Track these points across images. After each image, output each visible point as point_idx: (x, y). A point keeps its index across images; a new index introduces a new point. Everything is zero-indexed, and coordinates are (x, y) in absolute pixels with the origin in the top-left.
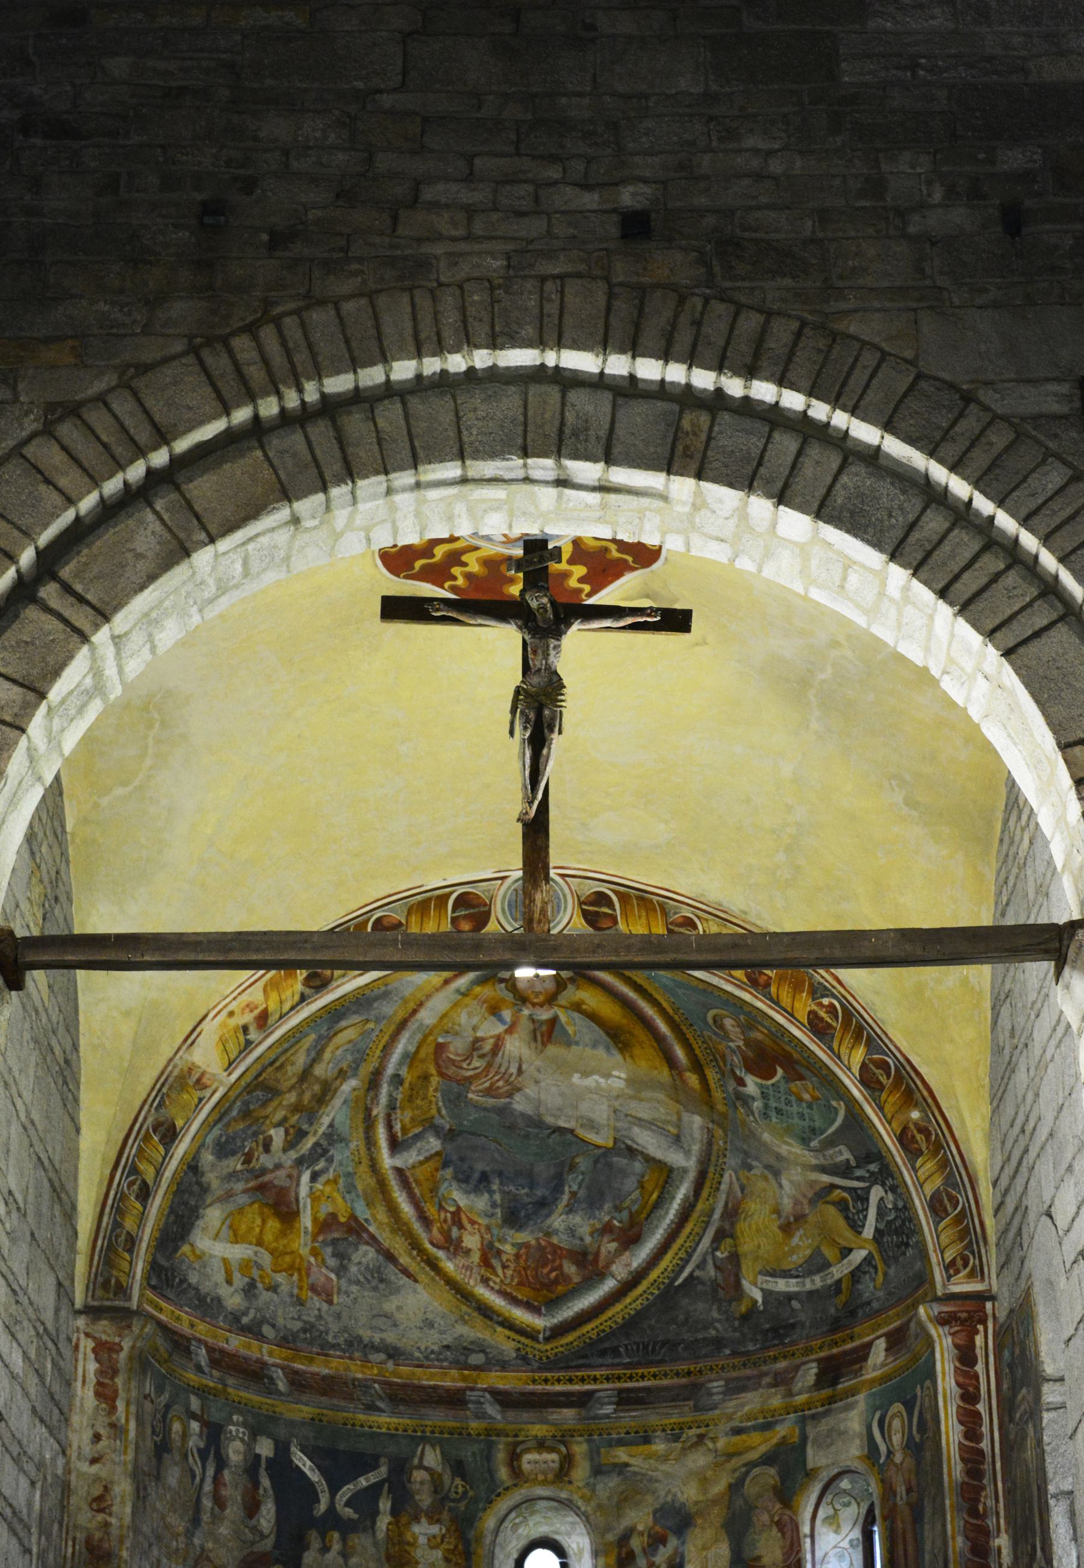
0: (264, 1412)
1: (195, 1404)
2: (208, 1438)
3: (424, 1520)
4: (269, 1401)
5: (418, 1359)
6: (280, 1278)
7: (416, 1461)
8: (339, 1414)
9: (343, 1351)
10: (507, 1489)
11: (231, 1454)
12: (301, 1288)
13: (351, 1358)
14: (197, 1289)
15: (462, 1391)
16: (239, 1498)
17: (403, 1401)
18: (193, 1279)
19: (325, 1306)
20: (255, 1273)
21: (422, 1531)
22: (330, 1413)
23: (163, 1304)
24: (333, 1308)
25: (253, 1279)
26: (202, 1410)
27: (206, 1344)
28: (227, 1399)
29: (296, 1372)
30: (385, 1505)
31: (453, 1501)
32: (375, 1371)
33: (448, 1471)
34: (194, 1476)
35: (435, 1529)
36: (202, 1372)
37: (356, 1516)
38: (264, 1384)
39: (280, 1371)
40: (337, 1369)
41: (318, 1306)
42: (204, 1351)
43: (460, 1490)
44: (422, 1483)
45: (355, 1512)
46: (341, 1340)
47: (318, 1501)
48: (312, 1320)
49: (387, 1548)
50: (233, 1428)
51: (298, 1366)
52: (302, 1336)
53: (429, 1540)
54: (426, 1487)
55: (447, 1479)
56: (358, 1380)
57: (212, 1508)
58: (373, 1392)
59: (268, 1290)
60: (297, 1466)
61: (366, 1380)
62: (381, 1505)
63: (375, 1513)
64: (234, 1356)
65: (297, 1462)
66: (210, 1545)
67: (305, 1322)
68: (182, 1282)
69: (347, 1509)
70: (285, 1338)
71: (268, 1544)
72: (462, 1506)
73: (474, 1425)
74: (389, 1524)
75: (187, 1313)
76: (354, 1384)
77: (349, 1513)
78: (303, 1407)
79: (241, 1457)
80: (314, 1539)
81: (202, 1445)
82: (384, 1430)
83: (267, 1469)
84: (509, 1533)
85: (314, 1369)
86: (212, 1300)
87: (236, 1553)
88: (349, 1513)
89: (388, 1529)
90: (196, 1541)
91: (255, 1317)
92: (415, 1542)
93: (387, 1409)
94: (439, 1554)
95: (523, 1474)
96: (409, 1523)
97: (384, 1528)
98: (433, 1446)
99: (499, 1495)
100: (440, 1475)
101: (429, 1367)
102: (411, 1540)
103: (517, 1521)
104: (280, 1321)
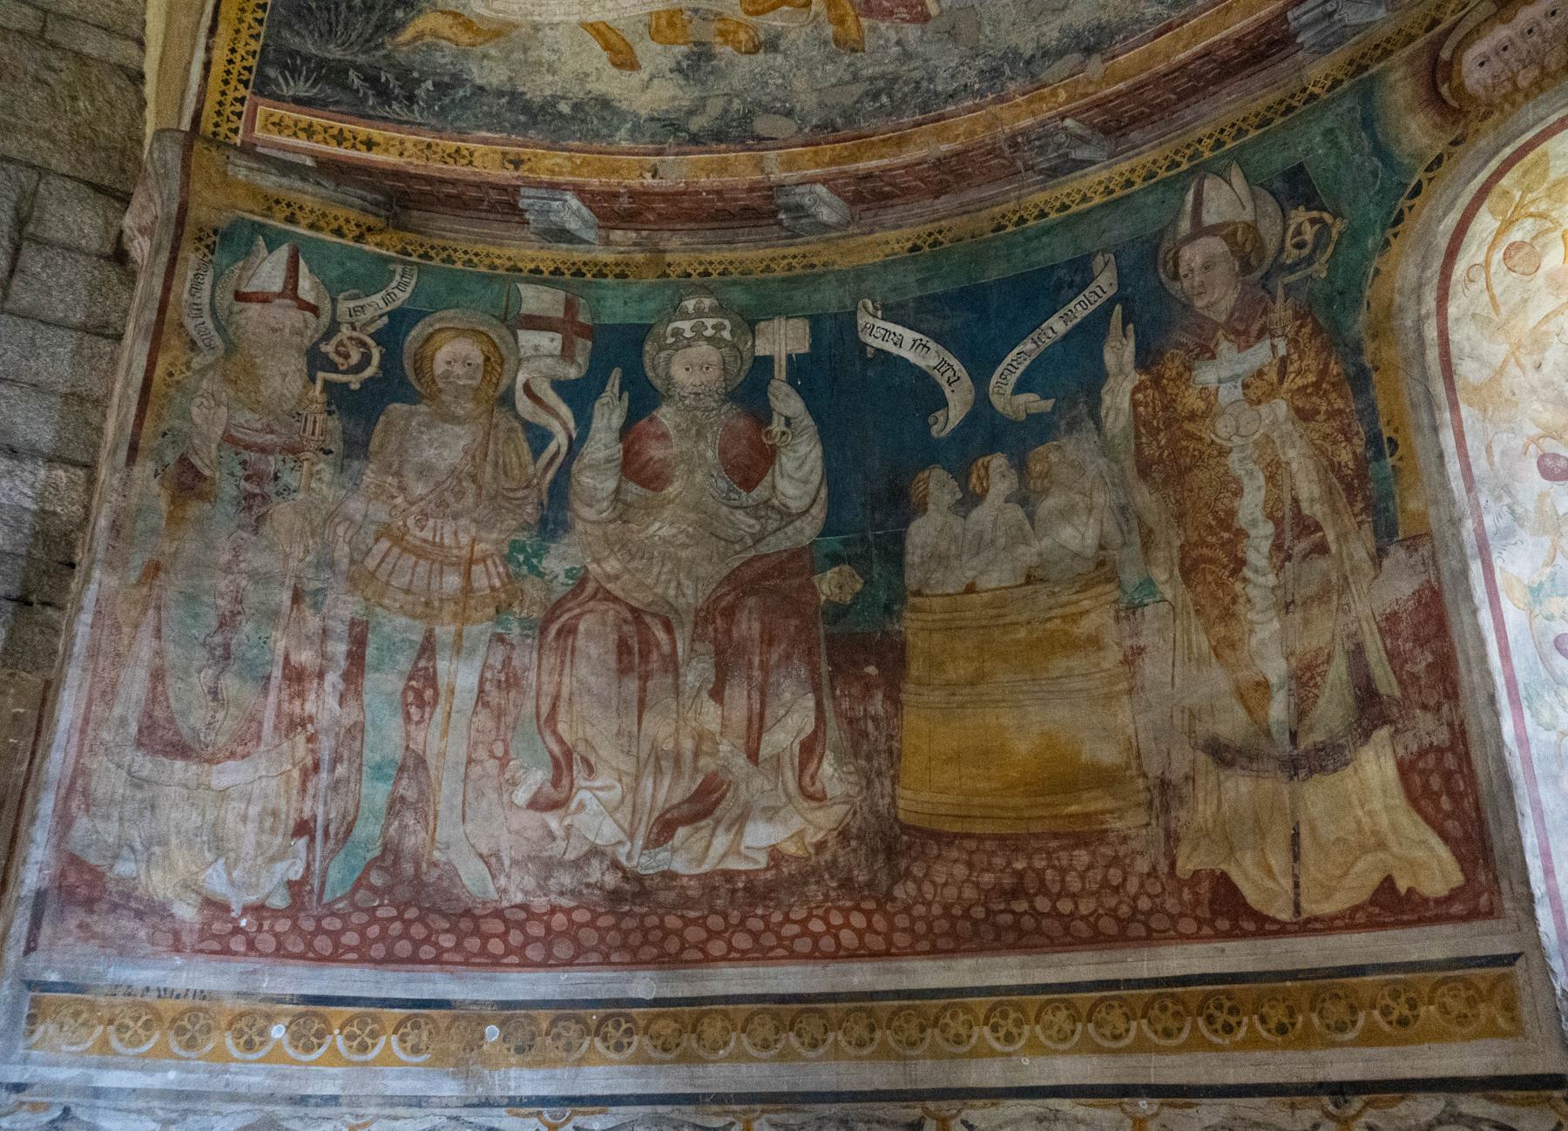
0: (779, 274)
1: (536, 299)
2: (594, 357)
3: (1224, 346)
4: (792, 251)
5: (1157, 18)
6: (775, 21)
7: (1185, 226)
8: (984, 214)
9: (975, 94)
10: (1439, 160)
11: (678, 373)
12: (840, 21)
13: (1001, 100)
14: (514, 96)
15: (1281, 16)
16: (710, 454)
17: (1134, 120)
18: (491, 73)
19: (912, 32)
20: (708, 32)
21: (1224, 374)
22: (957, 220)
23: (376, 134)
24: (930, 26)
25: (696, 44)
26: (570, 306)
27: (579, 191)
28: (665, 275)
29: (868, 176)
30: (1119, 353)
31: (1292, 269)
32: (1063, 96)
33: (1271, 207)
34: (539, 438)
35: (1260, 354)
36: (582, 241)
37: (1047, 405)
38: (780, 223)
39: (821, 189)
40: (972, 133)
41: (893, 37)
42: (574, 202)
43: (1309, 234)
44: (1206, 267)
45: (1045, 397)
46: (971, 76)
47: (944, 404)
48: (891, 68)
49: (1139, 447)
50: (686, 326)
51: (863, 166)
52: (869, 106)
53: (1245, 386)
54: (1221, 271)
55: (1270, 230)
56: (1023, 132)
57: (617, 491)
58: (1061, 138)
59: (754, 50)
60: (879, 351)
61: (1042, 124)
62: (1109, 358)
63: (1094, 381)
64: (669, 196)
65: (878, 344)
66: (612, 565)
67: (872, 79)
68: (442, 88)
69: (1023, 398)
70: (827, 126)
71: (807, 530)
72: (1320, 269)
73: (1318, 71)
74: (1136, 390)
75: (485, 141)
76: (1014, 145)
77: (1031, 402)
78: (892, 235)
79: (714, 373)
80: (938, 487)
81: (573, 373)
82: (1097, 200)
83: (791, 381)
84: (1502, 279)
85: (911, 154)
86: (577, 107)
87: (703, 570)
88: (1031, 402)
89: (1135, 404)
90: (557, 563)
91: (726, 111)
92: (1209, 406)
93: (1097, 155)
94: (1281, 407)
95: (1473, 99)
96: (1190, 369)
97: (1126, 404)
98: (1223, 175)
99: (1417, 191)
100: (1251, 227)
101: (1184, 20)
102: (1201, 405)
103: (1516, 235)
104: (805, 99)
